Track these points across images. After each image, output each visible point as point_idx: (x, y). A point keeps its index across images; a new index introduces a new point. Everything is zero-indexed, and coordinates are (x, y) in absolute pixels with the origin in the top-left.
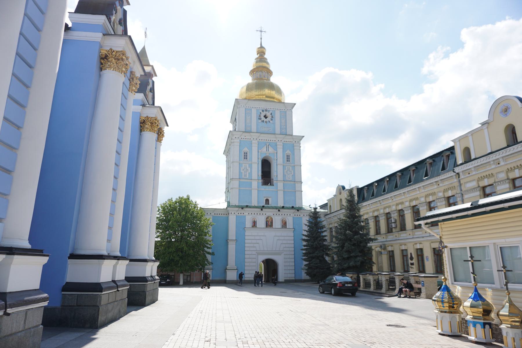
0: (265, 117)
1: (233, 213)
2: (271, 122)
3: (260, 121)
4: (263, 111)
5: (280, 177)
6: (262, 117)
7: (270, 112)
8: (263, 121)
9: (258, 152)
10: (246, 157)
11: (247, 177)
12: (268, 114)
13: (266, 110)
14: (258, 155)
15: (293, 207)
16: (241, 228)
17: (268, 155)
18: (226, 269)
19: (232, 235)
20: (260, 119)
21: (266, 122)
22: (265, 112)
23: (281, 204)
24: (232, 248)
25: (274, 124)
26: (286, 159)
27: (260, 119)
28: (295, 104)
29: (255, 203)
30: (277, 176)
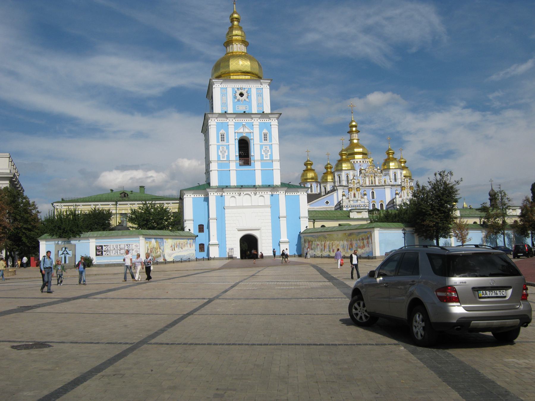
0: (241, 95)
2: (247, 100)
3: (236, 100)
8: (239, 100)
11: (225, 159)
12: (244, 92)
14: (235, 136)
16: (222, 208)
17: (244, 135)
18: (209, 244)
19: (213, 214)
23: (259, 182)
24: (213, 225)
25: (250, 102)
27: (235, 97)
29: (233, 182)
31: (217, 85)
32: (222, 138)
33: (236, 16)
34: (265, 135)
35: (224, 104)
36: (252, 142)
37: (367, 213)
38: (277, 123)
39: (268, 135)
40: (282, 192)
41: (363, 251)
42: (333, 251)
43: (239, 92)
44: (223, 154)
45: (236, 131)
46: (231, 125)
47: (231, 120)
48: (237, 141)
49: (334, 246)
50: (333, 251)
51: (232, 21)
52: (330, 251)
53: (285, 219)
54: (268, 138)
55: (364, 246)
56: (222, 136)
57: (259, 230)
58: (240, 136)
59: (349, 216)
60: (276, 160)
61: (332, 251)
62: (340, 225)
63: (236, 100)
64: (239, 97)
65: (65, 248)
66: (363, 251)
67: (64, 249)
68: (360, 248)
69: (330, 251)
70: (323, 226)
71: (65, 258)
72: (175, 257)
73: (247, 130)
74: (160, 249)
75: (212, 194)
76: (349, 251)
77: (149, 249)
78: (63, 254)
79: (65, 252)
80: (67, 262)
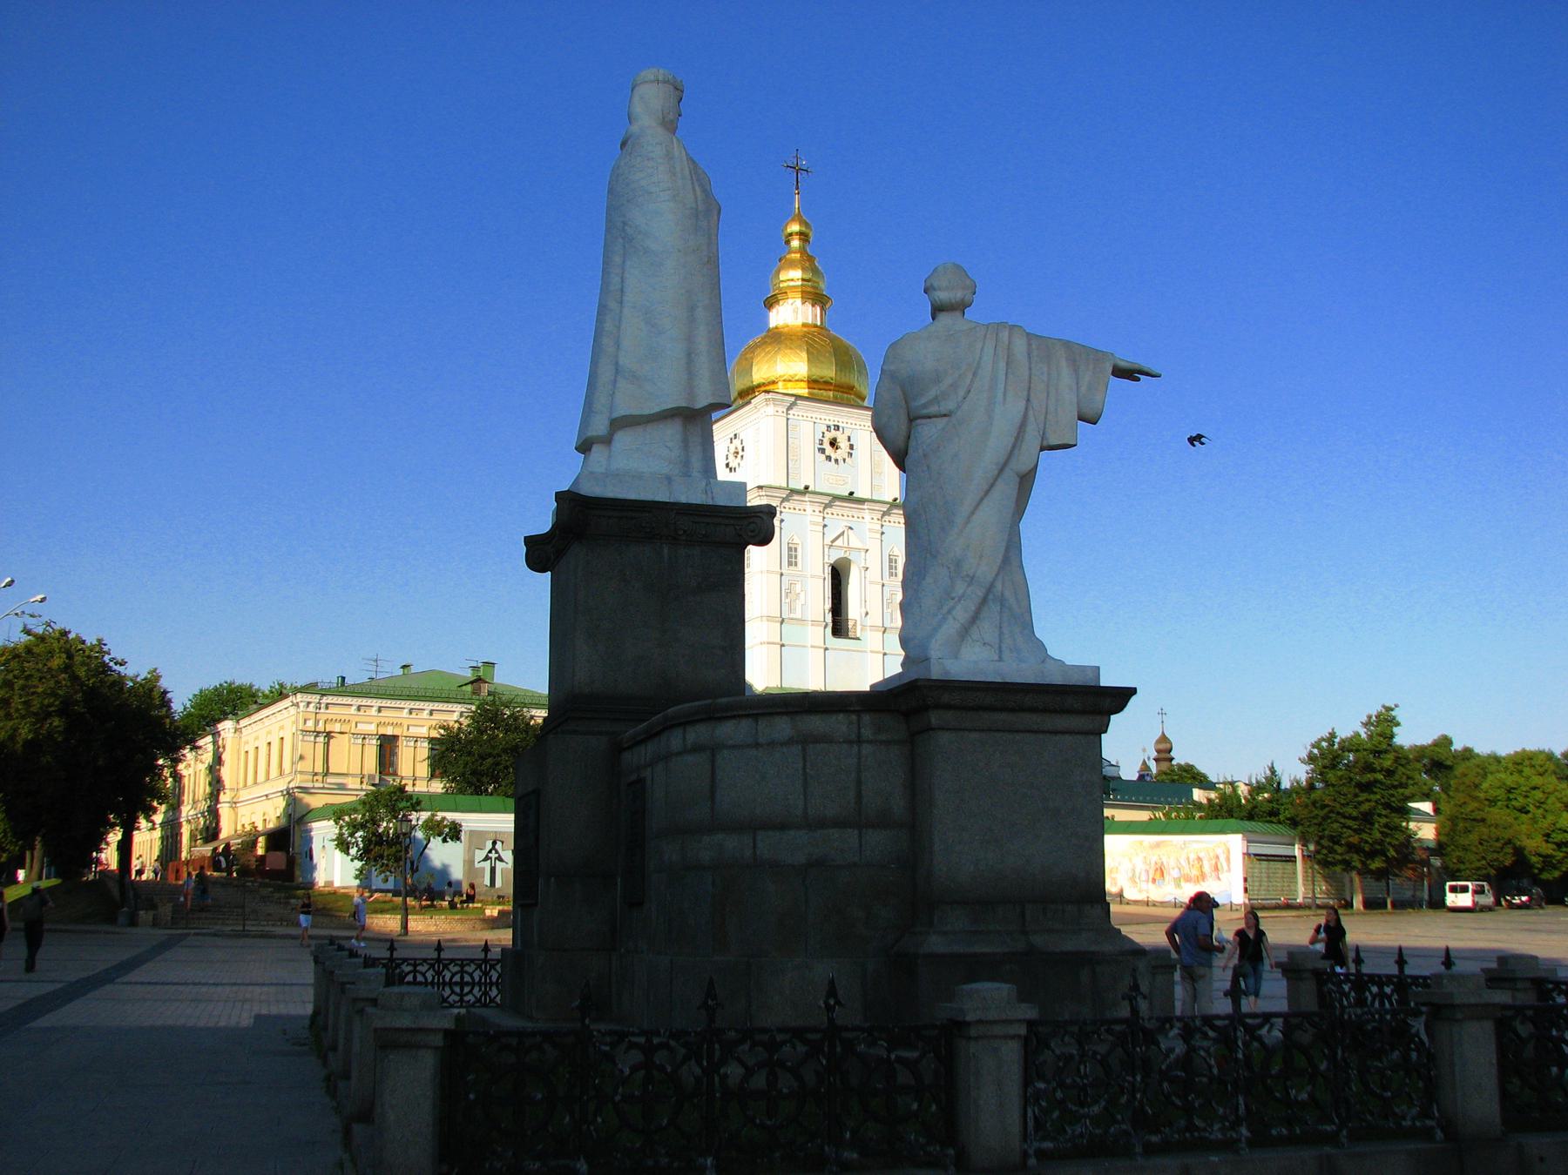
6: (826, 446)
7: (847, 433)
8: (829, 458)
10: (792, 562)
13: (837, 428)
20: (822, 451)
22: (833, 434)
27: (822, 451)
43: (829, 436)
48: (828, 570)
55: (1203, 877)
64: (829, 450)
65: (494, 843)
67: (489, 845)
68: (1188, 879)
71: (493, 870)
78: (487, 858)
79: (493, 855)
80: (498, 884)
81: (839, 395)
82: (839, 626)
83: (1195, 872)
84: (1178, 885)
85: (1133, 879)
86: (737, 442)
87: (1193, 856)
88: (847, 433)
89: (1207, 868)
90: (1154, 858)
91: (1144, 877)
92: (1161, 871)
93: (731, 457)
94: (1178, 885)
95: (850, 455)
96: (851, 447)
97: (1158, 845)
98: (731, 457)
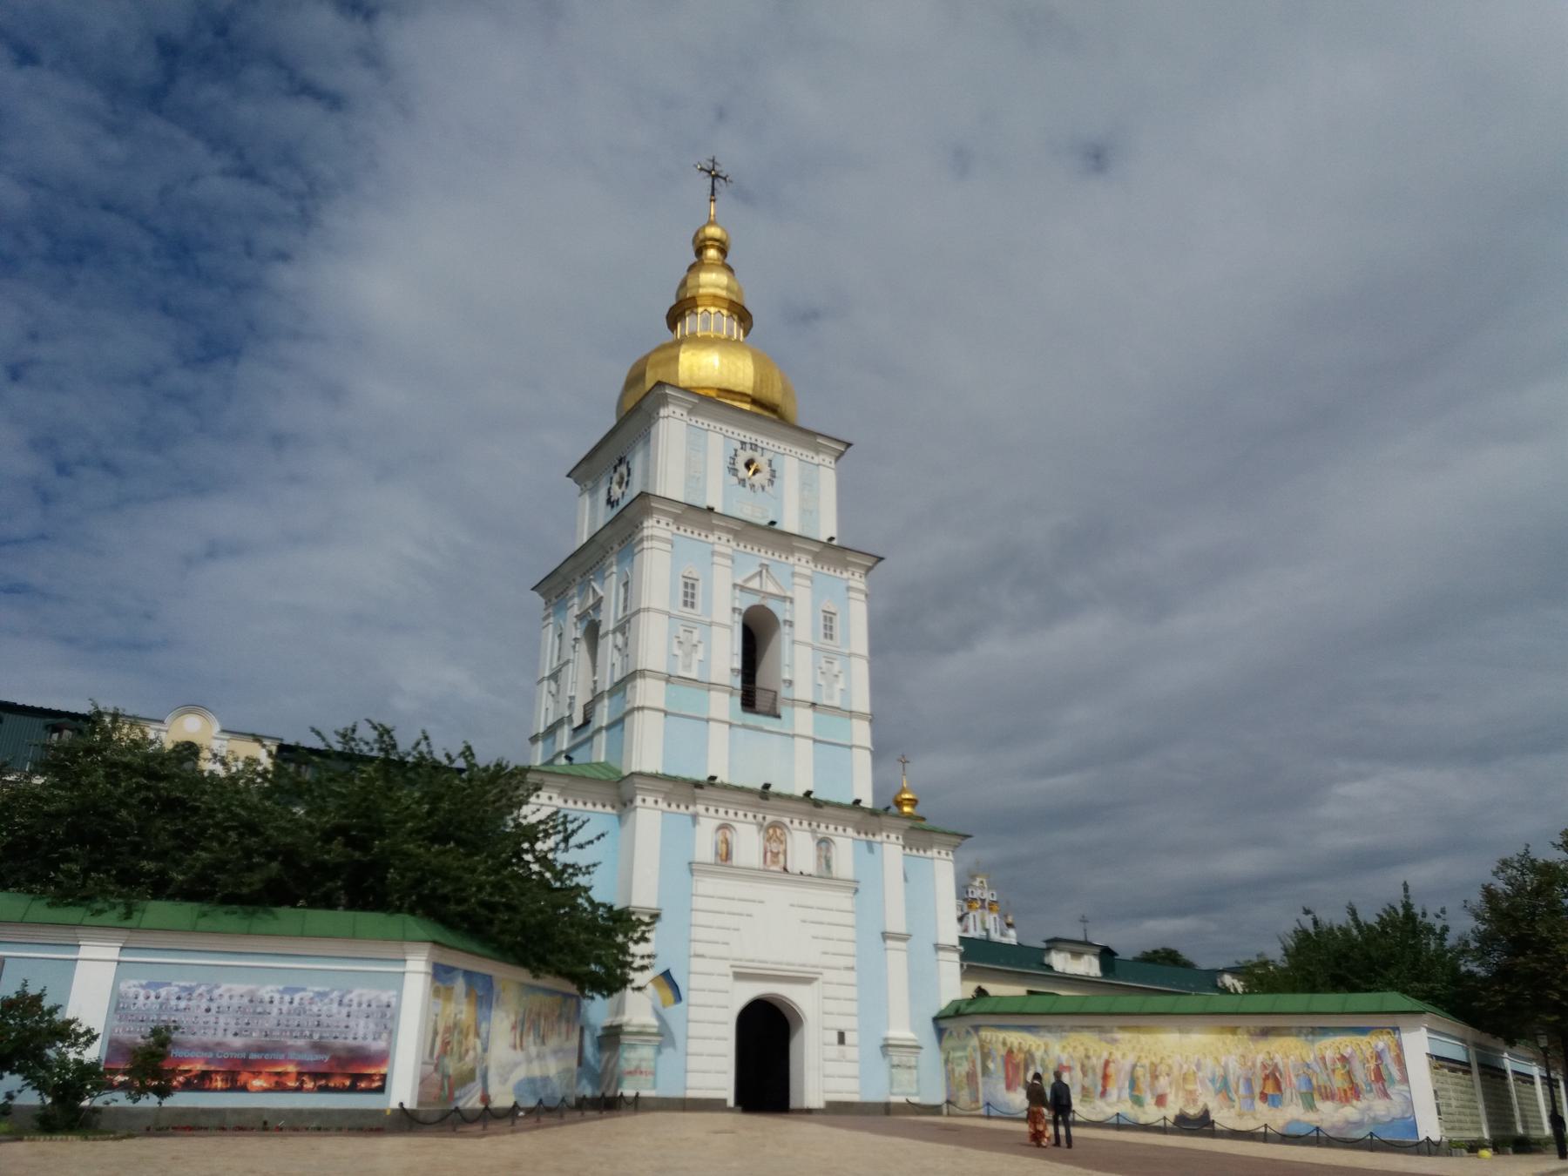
1: (650, 800)
3: (735, 480)
4: (743, 443)
5: (803, 691)
7: (768, 455)
8: (742, 482)
9: (735, 586)
12: (761, 461)
15: (857, 802)
17: (764, 602)
21: (753, 486)
26: (822, 631)
28: (849, 445)
30: (790, 683)
31: (679, 411)
32: (686, 594)
33: (713, 231)
34: (829, 617)
35: (695, 477)
36: (785, 629)
37: (1095, 962)
38: (862, 587)
39: (837, 621)
40: (893, 837)
41: (1351, 1112)
42: (1161, 1100)
43: (743, 457)
44: (688, 655)
45: (739, 581)
46: (723, 555)
47: (725, 537)
48: (738, 619)
49: (1163, 1081)
50: (1161, 1100)
51: (700, 251)
52: (1137, 1101)
53: (901, 945)
54: (837, 631)
55: (1354, 1092)
56: (690, 587)
57: (807, 981)
58: (755, 600)
59: (1050, 968)
60: (861, 716)
61: (1149, 1100)
62: (1030, 993)
63: (735, 480)
66: (1351, 1112)
68: (1328, 1096)
69: (1137, 1101)
70: (981, 992)
72: (518, 1088)
73: (771, 588)
74: (477, 1035)
75: (650, 800)
76: (1260, 1106)
77: (441, 1030)
81: (756, 409)
82: (753, 693)
83: (1339, 1082)
84: (1310, 1106)
85: (1224, 1088)
86: (623, 469)
87: (1329, 1054)
88: (768, 455)
89: (1361, 1076)
90: (1260, 1058)
91: (1242, 1090)
92: (1273, 1077)
93: (615, 487)
94: (1310, 1106)
95: (771, 482)
96: (773, 473)
97: (1266, 1033)
98: (615, 487)
